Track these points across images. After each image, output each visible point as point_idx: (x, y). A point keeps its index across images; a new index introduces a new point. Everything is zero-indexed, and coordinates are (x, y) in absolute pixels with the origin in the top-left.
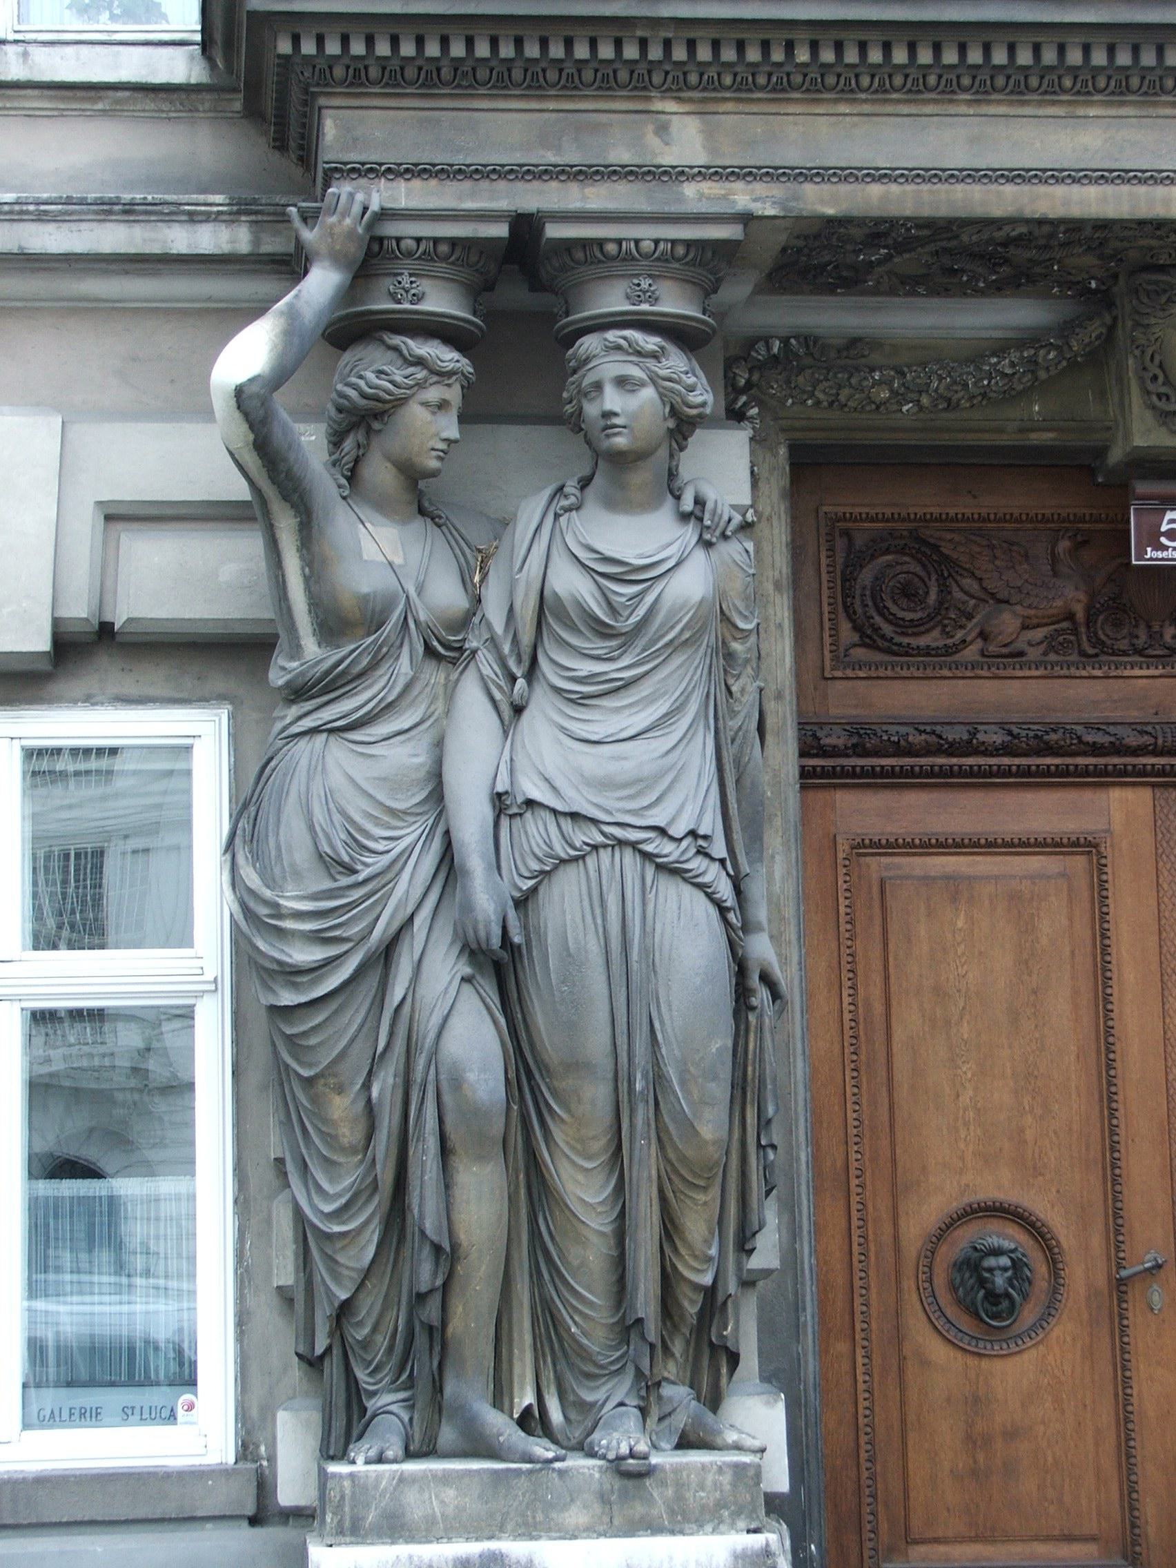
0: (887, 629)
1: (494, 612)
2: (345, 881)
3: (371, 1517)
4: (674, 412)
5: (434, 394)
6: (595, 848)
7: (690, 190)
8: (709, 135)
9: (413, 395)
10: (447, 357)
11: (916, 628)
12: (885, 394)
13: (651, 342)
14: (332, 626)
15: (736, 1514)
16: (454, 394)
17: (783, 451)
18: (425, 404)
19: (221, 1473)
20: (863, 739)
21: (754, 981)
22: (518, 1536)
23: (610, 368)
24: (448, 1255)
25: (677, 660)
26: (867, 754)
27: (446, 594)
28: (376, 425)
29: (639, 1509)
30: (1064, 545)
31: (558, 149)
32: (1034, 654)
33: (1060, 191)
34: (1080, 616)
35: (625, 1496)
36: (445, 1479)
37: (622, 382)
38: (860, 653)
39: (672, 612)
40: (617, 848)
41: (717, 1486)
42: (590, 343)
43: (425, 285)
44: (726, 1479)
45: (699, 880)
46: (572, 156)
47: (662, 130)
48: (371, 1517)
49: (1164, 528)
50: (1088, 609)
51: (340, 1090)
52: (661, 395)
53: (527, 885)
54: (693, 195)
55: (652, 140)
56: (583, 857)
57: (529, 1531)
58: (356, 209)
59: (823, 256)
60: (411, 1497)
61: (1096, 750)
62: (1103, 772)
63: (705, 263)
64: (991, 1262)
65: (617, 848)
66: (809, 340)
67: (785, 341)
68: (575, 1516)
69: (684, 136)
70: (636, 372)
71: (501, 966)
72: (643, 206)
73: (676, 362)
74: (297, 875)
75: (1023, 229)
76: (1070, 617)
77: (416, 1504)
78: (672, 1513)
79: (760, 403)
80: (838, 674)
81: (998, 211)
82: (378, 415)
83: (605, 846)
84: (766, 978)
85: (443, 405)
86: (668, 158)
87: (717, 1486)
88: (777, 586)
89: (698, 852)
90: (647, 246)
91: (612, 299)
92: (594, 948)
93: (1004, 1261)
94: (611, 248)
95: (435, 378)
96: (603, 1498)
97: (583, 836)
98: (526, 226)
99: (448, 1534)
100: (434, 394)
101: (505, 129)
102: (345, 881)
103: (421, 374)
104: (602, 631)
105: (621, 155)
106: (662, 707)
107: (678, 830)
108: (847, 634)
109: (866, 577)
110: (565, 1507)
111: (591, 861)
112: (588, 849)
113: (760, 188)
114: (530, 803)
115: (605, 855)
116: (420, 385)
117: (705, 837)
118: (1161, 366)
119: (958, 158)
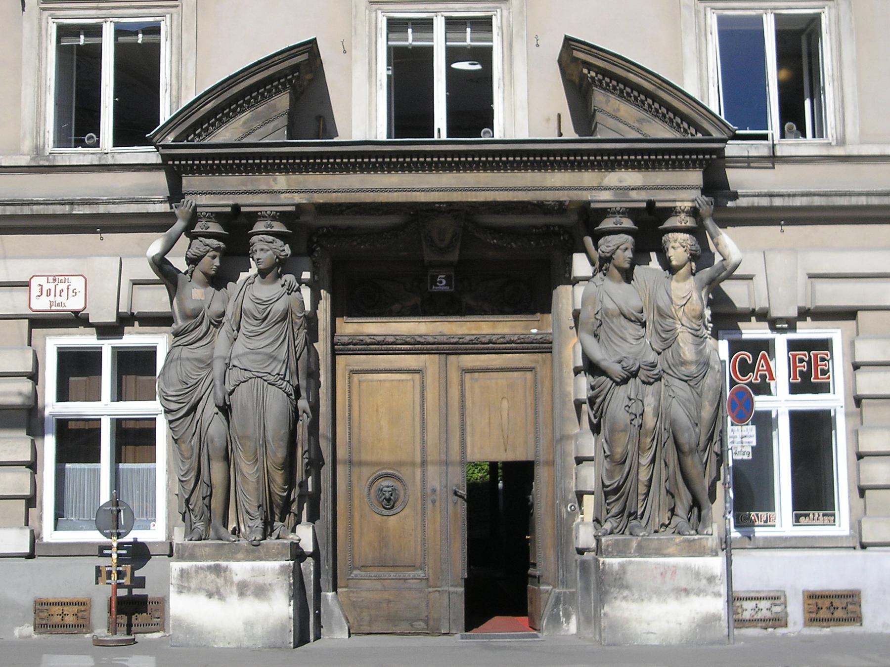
1: (229, 313)
2: (186, 386)
5: (214, 253)
7: (282, 196)
8: (288, 181)
10: (214, 243)
13: (270, 238)
14: (186, 317)
19: (162, 543)
21: (300, 413)
22: (224, 561)
23: (258, 246)
24: (210, 486)
27: (217, 307)
29: (257, 554)
31: (246, 186)
35: (253, 551)
36: (206, 546)
37: (262, 250)
41: (278, 549)
42: (255, 239)
43: (209, 224)
46: (250, 188)
51: (184, 442)
53: (232, 388)
54: (284, 198)
55: (272, 183)
58: (189, 205)
60: (197, 550)
63: (282, 217)
66: (334, 227)
69: (281, 181)
70: (266, 247)
71: (225, 410)
72: (269, 202)
73: (279, 243)
74: (173, 385)
77: (198, 552)
79: (321, 246)
81: (368, 200)
85: (214, 257)
87: (278, 549)
92: (250, 405)
93: (390, 489)
96: (247, 551)
97: (248, 374)
98: (236, 208)
99: (206, 560)
100: (211, 254)
101: (232, 181)
102: (186, 386)
103: (208, 248)
104: (256, 319)
105: (263, 187)
106: (272, 339)
116: (208, 252)
119: (357, 186)
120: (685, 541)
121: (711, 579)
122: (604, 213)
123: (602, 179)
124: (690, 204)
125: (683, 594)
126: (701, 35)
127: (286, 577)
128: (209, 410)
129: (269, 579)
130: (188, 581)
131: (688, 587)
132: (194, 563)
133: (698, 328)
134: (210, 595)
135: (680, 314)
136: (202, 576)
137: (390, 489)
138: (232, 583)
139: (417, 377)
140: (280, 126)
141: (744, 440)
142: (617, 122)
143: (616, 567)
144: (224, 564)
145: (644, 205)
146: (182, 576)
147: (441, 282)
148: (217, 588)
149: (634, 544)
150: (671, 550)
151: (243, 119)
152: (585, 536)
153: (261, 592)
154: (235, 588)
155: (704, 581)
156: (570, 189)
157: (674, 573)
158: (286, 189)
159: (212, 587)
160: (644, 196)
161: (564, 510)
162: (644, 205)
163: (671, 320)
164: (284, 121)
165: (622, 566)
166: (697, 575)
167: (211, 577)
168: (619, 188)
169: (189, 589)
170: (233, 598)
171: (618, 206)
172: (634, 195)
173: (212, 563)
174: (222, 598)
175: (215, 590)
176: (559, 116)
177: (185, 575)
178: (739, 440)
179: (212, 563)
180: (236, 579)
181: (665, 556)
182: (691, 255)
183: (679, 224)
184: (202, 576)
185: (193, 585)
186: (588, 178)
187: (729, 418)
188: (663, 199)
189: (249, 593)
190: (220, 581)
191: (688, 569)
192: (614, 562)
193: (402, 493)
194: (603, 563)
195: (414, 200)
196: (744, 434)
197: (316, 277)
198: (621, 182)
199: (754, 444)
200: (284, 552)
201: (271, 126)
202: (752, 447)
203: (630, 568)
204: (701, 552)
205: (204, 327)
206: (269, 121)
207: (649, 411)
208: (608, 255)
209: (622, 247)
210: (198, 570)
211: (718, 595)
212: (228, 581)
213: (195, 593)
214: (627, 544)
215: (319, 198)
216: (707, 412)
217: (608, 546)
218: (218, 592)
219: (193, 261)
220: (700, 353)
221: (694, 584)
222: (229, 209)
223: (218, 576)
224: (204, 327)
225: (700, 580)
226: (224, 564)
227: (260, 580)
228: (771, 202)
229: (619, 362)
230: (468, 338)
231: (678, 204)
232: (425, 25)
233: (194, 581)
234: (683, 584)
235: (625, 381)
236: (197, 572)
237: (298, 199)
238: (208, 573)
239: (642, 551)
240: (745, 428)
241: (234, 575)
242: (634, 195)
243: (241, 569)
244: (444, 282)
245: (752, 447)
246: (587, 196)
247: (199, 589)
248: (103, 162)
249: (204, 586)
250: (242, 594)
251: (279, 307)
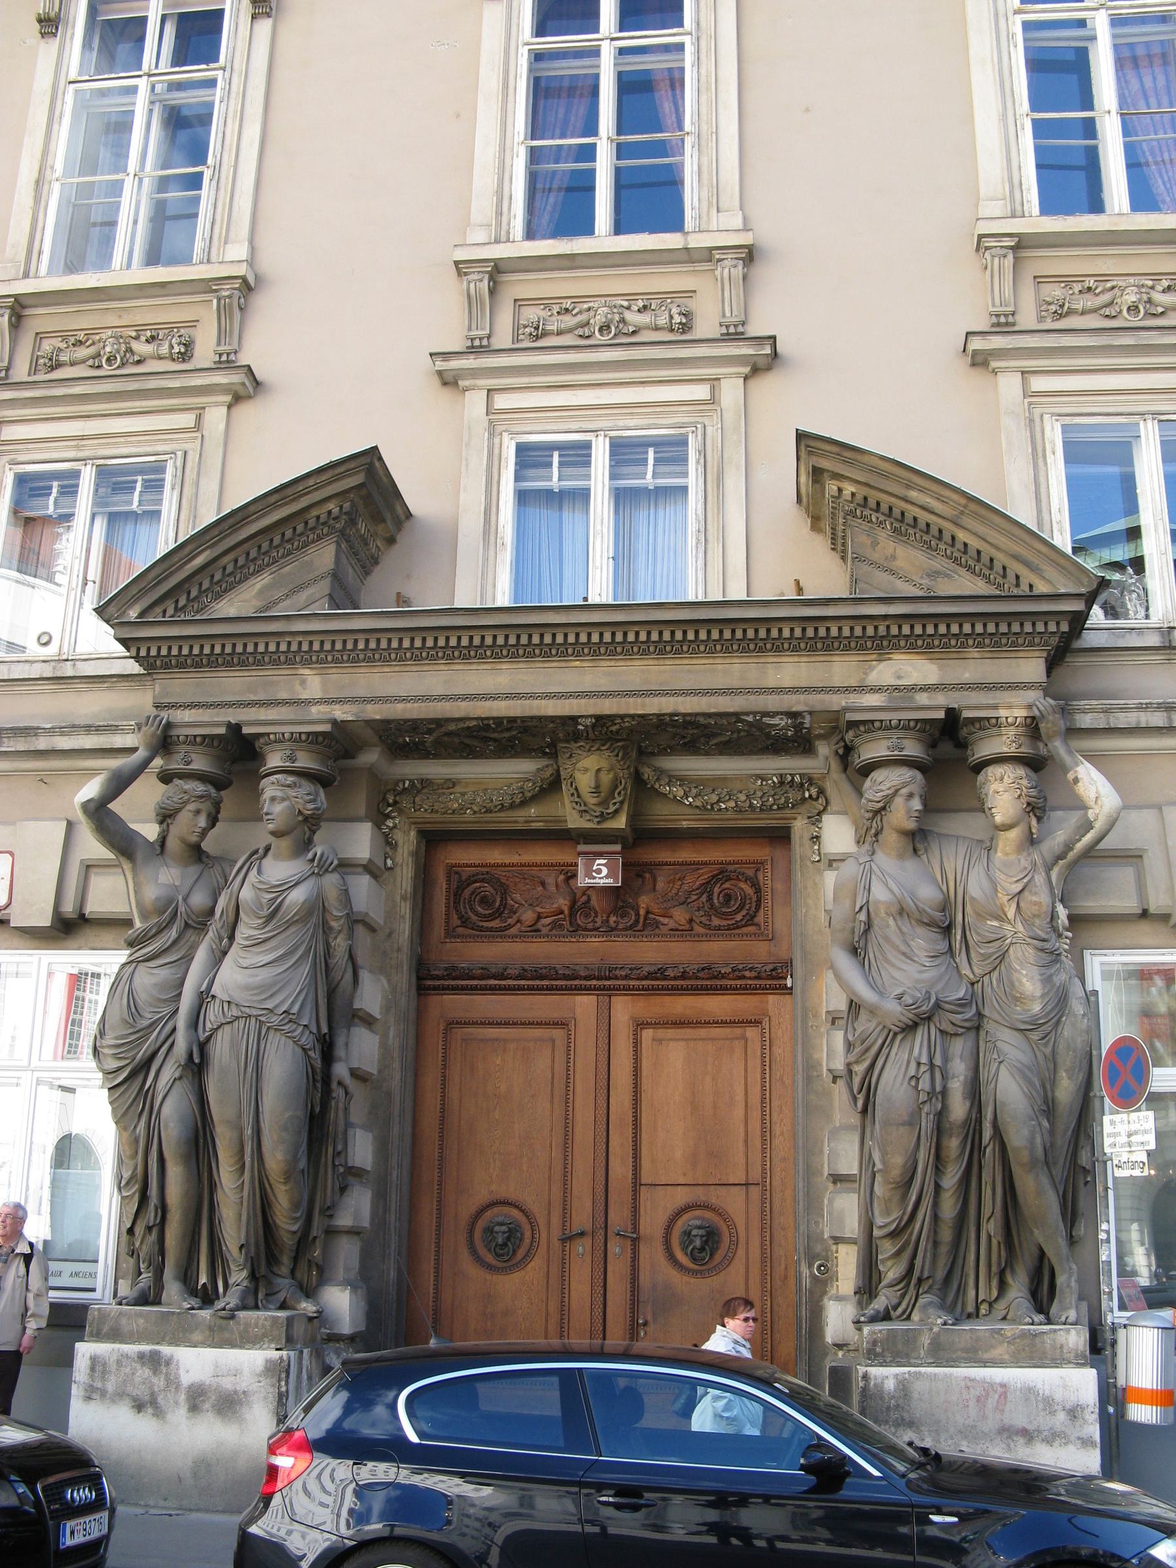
0: (474, 918)
3: (105, 1329)
6: (238, 1018)
7: (314, 709)
8: (324, 684)
11: (491, 917)
12: (456, 805)
13: (291, 779)
15: (270, 1341)
17: (413, 833)
20: (453, 972)
21: (334, 1085)
22: (170, 1344)
23: (269, 793)
24: (163, 1207)
25: (293, 929)
26: (454, 979)
27: (199, 899)
29: (227, 1335)
30: (562, 877)
32: (545, 931)
33: (488, 704)
34: (566, 912)
38: (460, 930)
39: (289, 907)
41: (263, 1326)
43: (193, 756)
44: (268, 1323)
47: (303, 683)
48: (105, 1329)
50: (571, 908)
54: (316, 711)
55: (298, 688)
57: (175, 1342)
58: (157, 722)
59: (411, 738)
60: (124, 1321)
61: (566, 977)
62: (567, 988)
64: (497, 1228)
67: (411, 781)
68: (197, 1336)
75: (474, 723)
76: (562, 912)
78: (242, 1338)
82: (170, 816)
84: (340, 1083)
86: (304, 696)
87: (263, 1326)
88: (404, 898)
93: (504, 1228)
96: (211, 1329)
100: (192, 807)
101: (232, 684)
105: (283, 695)
108: (456, 921)
109: (467, 892)
110: (192, 1332)
113: (347, 707)
115: (242, 1021)
116: (186, 803)
118: (576, 789)
119: (440, 690)
120: (1023, 1335)
121: (1074, 1413)
122: (868, 726)
123: (865, 673)
124: (1023, 713)
125: (1021, 1441)
126: (1037, 455)
127: (275, 1380)
128: (168, 1072)
129: (246, 1382)
130: (103, 1379)
131: (1030, 1427)
132: (117, 1346)
133: (1046, 937)
134: (139, 1407)
135: (1011, 912)
136: (128, 1370)
137: (504, 1228)
138: (178, 1386)
139: (558, 1034)
140: (318, 596)
141: (1134, 1139)
142: (892, 578)
143: (890, 1385)
144: (166, 1350)
145: (941, 715)
146: (92, 1369)
147: (599, 871)
148: (153, 1394)
149: (925, 1340)
150: (1000, 1351)
151: (258, 586)
152: (838, 1318)
153: (229, 1404)
154: (182, 1397)
155: (1062, 1416)
156: (807, 690)
157: (1004, 1395)
158: (318, 695)
159: (142, 1392)
160: (941, 699)
161: (805, 1271)
162: (941, 715)
163: (995, 923)
164: (324, 587)
165: (904, 1386)
166: (1048, 1404)
167: (144, 1372)
168: (897, 688)
169: (103, 1393)
170: (179, 1415)
171: (895, 716)
172: (923, 699)
173: (146, 1348)
174: (159, 1413)
175: (147, 1398)
176: (797, 582)
177: (98, 1368)
178: (1123, 1139)
179: (146, 1348)
180: (186, 1379)
181: (985, 1364)
182: (1029, 804)
183: (1005, 749)
184: (128, 1370)
185: (110, 1387)
186: (841, 669)
187: (1107, 1100)
188: (971, 705)
189: (207, 1406)
190: (159, 1382)
191: (1029, 1392)
192: (886, 1376)
193: (528, 1234)
194: (865, 1377)
195: (535, 713)
196: (1133, 1127)
197: (389, 862)
198: (899, 677)
199: (1152, 1146)
200: (276, 1333)
201: (303, 596)
202: (1149, 1153)
203: (918, 1387)
204: (1057, 1361)
205: (173, 933)
206: (301, 587)
207: (957, 1087)
209: (904, 791)
210: (122, 1360)
211: (1086, 1442)
212: (173, 1383)
213: (113, 1401)
214: (911, 1338)
215: (375, 712)
216: (1066, 1090)
217: (875, 1343)
218: (153, 1402)
219: (166, 817)
220: (1047, 980)
221: (1044, 1422)
222: (222, 730)
223: (156, 1371)
224: (173, 933)
225: (1053, 1413)
226: (166, 1350)
227: (227, 1384)
228: (1170, 719)
229: (899, 998)
230: (647, 969)
231: (1003, 713)
232: (578, 454)
233: (113, 1378)
234: (1020, 1421)
235: (910, 1028)
236: (119, 1363)
237: (341, 713)
238: (138, 1366)
239: (941, 1354)
240: (1134, 1116)
241: (182, 1372)
242: (923, 699)
243: (195, 1362)
244: (605, 871)
245: (1149, 1153)
246: (837, 702)
247: (120, 1395)
248: (59, 674)
249: (129, 1389)
250: (194, 1408)
251: (297, 896)
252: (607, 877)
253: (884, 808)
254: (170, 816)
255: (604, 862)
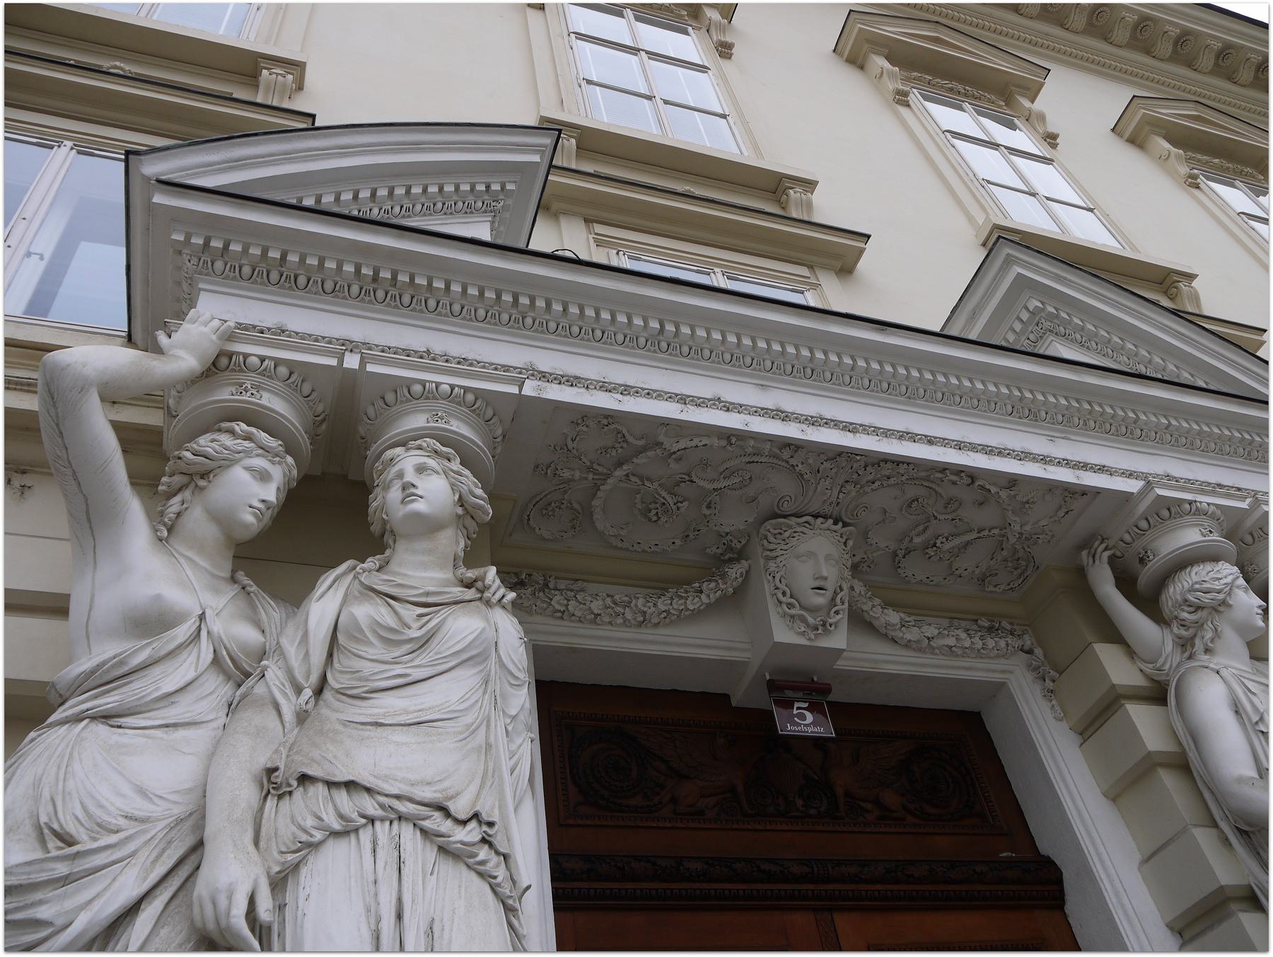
4: (461, 502)
5: (260, 462)
6: (372, 821)
9: (240, 460)
16: (277, 473)
18: (247, 469)
28: (202, 483)
40: (396, 823)
45: (481, 868)
49: (795, 712)
52: (452, 485)
56: (356, 830)
65: (396, 823)
80: (571, 822)
83: (382, 820)
85: (263, 477)
89: (484, 840)
90: (446, 388)
91: (418, 421)
94: (417, 388)
95: (260, 451)
107: (460, 808)
111: (365, 835)
112: (364, 821)
114: (304, 779)
115: (382, 829)
116: (248, 453)
117: (491, 824)
147: (803, 718)
208: (1221, 596)
252: (814, 724)
253: (1224, 603)
254: (204, 476)
255: (806, 705)
